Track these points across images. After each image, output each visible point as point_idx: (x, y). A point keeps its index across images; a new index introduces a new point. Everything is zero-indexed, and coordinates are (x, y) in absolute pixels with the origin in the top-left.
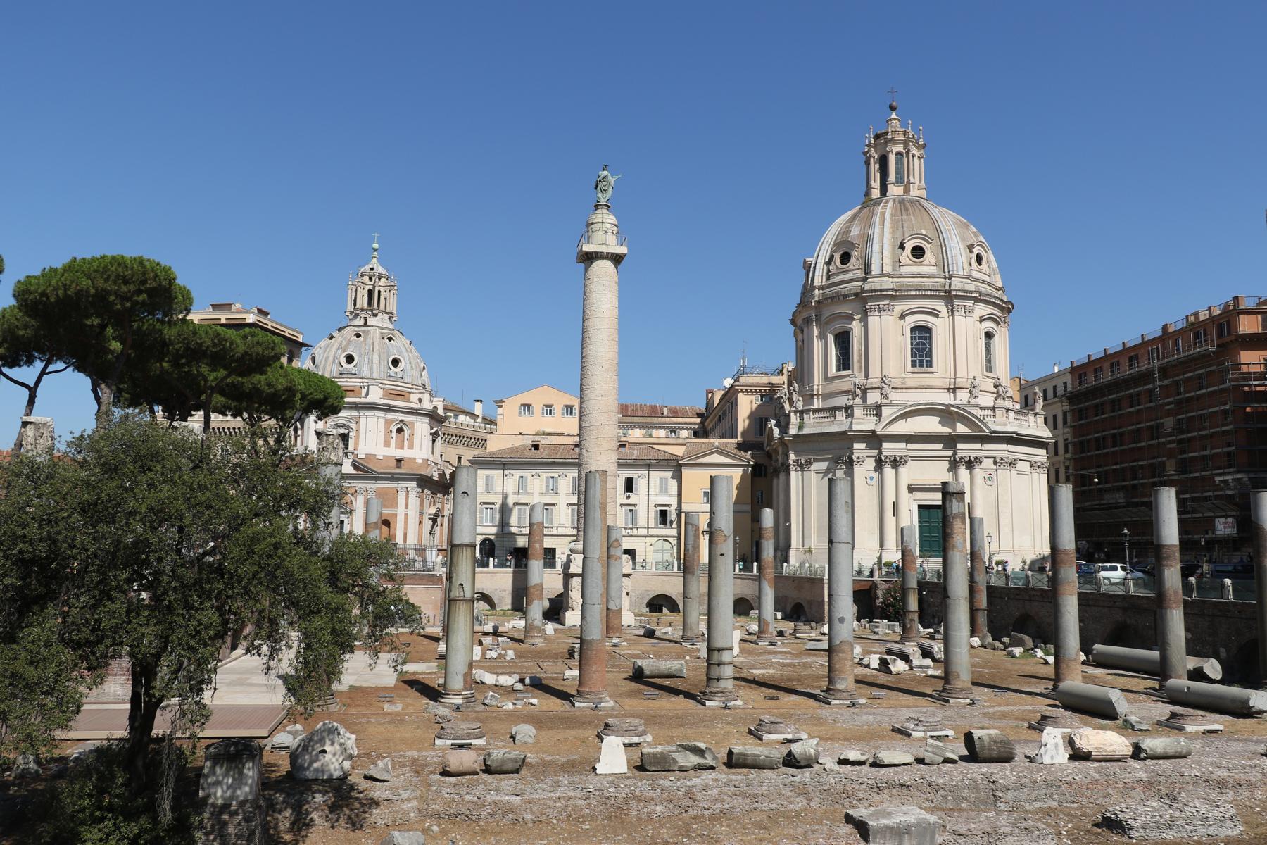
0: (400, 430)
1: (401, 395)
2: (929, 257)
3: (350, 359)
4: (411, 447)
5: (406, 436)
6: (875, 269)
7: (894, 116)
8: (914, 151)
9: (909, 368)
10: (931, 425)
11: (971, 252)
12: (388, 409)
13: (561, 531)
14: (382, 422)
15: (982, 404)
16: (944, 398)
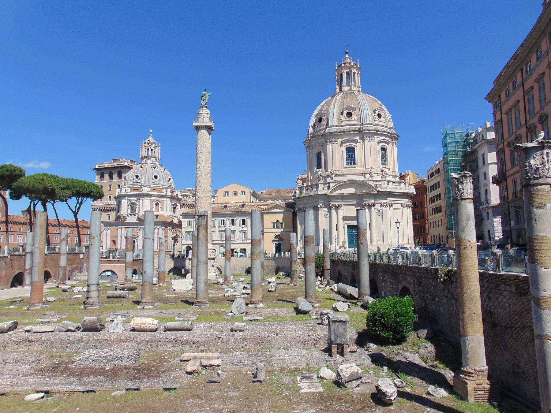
0: (157, 204)
1: (158, 190)
2: (354, 116)
3: (137, 177)
4: (162, 210)
5: (160, 206)
6: (330, 124)
7: (347, 56)
8: (354, 71)
9: (345, 165)
10: (351, 191)
11: (375, 113)
12: (150, 196)
13: (217, 242)
14: (149, 201)
15: (374, 179)
16: (360, 178)
